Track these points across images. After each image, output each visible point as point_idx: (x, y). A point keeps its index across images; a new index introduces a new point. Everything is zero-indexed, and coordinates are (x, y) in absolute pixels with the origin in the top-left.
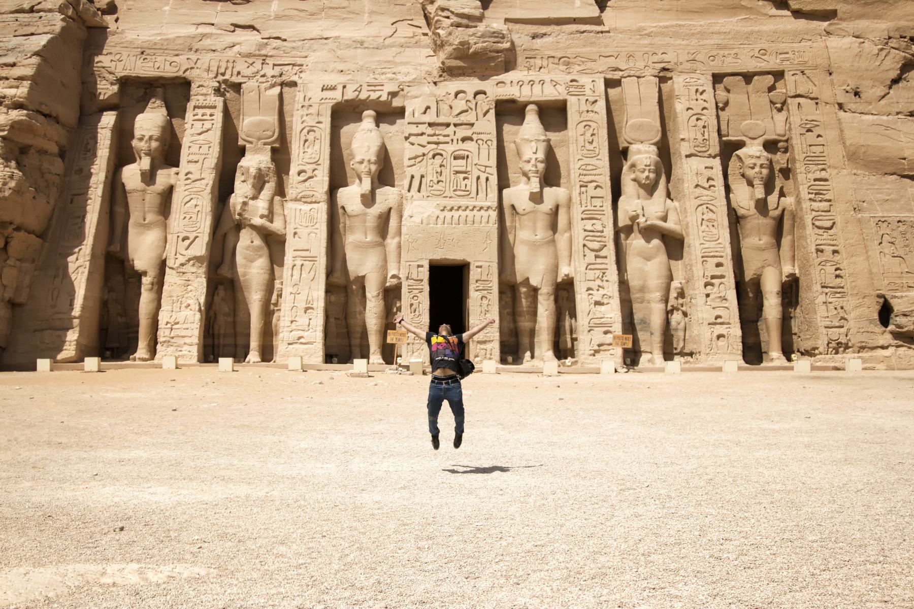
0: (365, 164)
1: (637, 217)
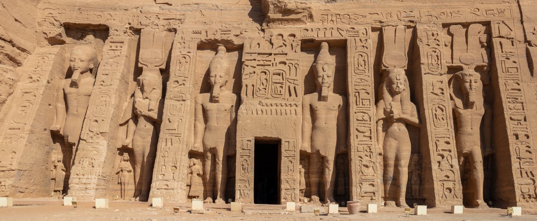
0: (218, 77)
1: (392, 112)
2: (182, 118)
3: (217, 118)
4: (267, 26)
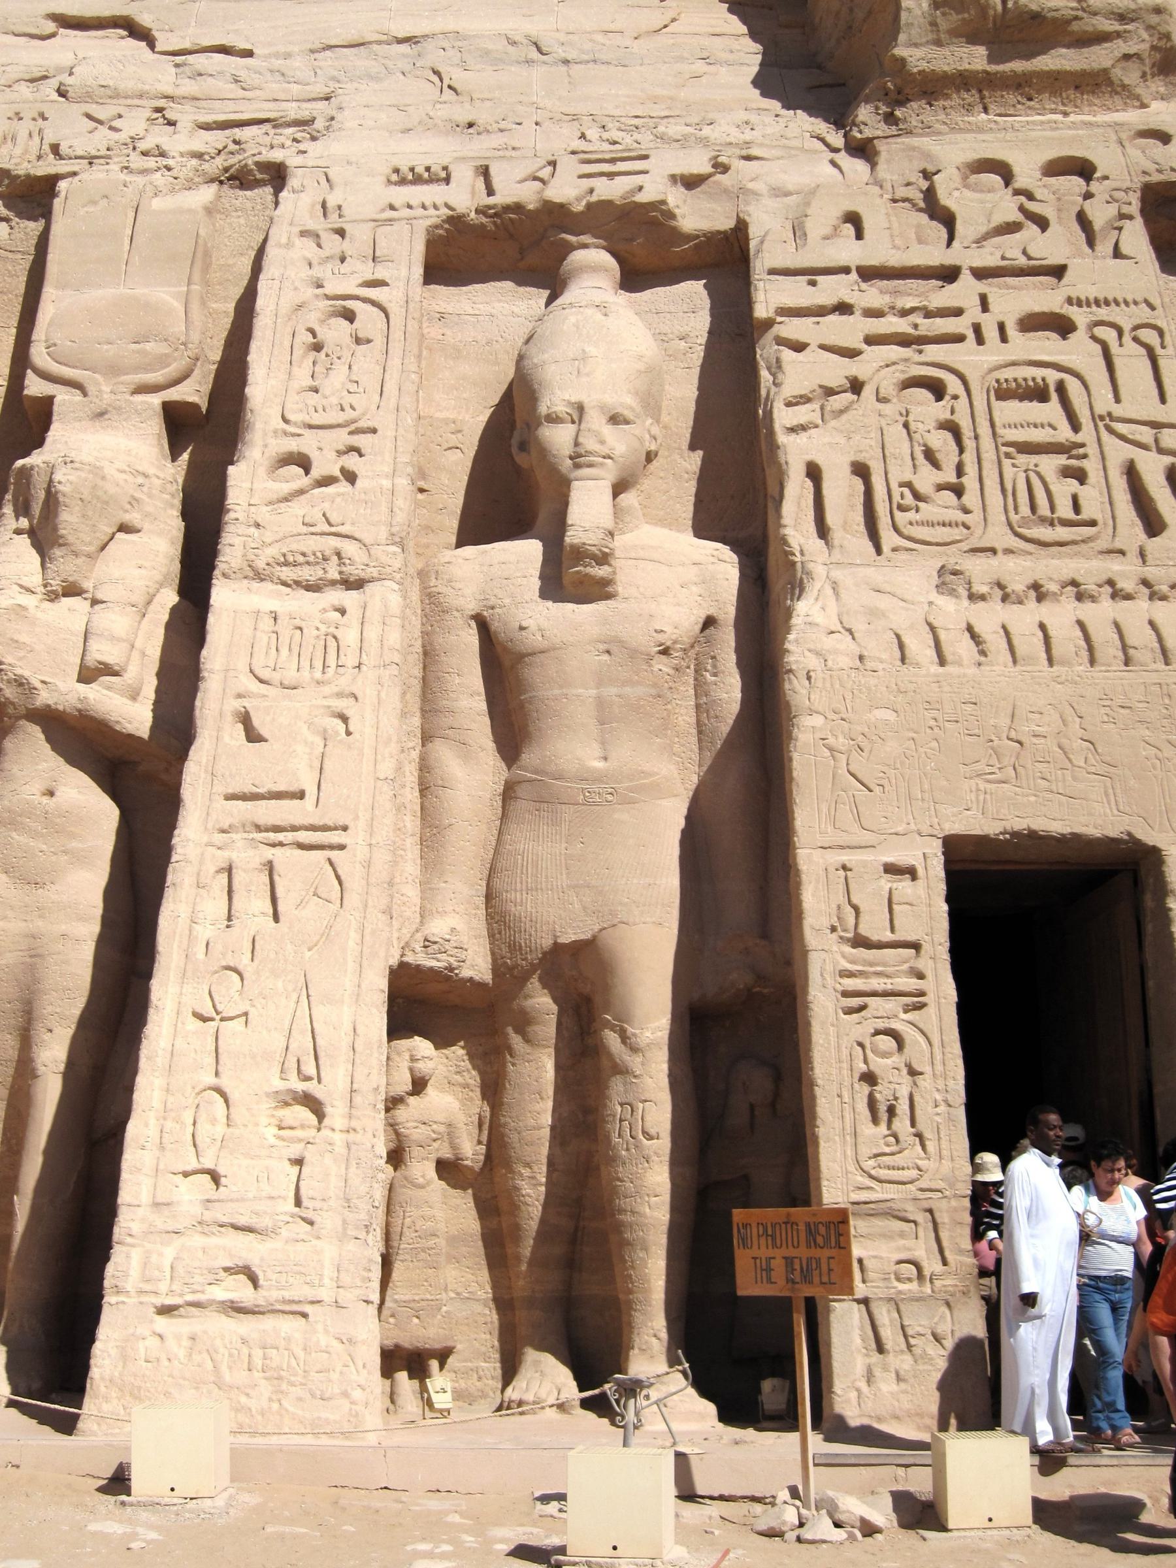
0: (595, 421)
2: (341, 705)
3: (604, 715)
4: (890, 119)
